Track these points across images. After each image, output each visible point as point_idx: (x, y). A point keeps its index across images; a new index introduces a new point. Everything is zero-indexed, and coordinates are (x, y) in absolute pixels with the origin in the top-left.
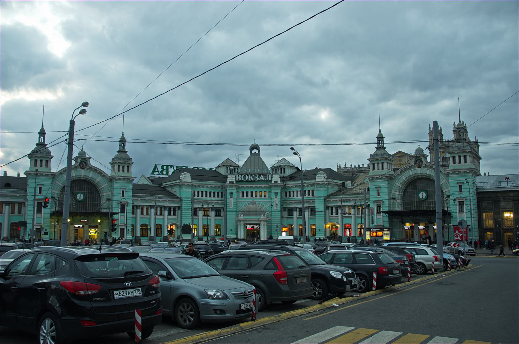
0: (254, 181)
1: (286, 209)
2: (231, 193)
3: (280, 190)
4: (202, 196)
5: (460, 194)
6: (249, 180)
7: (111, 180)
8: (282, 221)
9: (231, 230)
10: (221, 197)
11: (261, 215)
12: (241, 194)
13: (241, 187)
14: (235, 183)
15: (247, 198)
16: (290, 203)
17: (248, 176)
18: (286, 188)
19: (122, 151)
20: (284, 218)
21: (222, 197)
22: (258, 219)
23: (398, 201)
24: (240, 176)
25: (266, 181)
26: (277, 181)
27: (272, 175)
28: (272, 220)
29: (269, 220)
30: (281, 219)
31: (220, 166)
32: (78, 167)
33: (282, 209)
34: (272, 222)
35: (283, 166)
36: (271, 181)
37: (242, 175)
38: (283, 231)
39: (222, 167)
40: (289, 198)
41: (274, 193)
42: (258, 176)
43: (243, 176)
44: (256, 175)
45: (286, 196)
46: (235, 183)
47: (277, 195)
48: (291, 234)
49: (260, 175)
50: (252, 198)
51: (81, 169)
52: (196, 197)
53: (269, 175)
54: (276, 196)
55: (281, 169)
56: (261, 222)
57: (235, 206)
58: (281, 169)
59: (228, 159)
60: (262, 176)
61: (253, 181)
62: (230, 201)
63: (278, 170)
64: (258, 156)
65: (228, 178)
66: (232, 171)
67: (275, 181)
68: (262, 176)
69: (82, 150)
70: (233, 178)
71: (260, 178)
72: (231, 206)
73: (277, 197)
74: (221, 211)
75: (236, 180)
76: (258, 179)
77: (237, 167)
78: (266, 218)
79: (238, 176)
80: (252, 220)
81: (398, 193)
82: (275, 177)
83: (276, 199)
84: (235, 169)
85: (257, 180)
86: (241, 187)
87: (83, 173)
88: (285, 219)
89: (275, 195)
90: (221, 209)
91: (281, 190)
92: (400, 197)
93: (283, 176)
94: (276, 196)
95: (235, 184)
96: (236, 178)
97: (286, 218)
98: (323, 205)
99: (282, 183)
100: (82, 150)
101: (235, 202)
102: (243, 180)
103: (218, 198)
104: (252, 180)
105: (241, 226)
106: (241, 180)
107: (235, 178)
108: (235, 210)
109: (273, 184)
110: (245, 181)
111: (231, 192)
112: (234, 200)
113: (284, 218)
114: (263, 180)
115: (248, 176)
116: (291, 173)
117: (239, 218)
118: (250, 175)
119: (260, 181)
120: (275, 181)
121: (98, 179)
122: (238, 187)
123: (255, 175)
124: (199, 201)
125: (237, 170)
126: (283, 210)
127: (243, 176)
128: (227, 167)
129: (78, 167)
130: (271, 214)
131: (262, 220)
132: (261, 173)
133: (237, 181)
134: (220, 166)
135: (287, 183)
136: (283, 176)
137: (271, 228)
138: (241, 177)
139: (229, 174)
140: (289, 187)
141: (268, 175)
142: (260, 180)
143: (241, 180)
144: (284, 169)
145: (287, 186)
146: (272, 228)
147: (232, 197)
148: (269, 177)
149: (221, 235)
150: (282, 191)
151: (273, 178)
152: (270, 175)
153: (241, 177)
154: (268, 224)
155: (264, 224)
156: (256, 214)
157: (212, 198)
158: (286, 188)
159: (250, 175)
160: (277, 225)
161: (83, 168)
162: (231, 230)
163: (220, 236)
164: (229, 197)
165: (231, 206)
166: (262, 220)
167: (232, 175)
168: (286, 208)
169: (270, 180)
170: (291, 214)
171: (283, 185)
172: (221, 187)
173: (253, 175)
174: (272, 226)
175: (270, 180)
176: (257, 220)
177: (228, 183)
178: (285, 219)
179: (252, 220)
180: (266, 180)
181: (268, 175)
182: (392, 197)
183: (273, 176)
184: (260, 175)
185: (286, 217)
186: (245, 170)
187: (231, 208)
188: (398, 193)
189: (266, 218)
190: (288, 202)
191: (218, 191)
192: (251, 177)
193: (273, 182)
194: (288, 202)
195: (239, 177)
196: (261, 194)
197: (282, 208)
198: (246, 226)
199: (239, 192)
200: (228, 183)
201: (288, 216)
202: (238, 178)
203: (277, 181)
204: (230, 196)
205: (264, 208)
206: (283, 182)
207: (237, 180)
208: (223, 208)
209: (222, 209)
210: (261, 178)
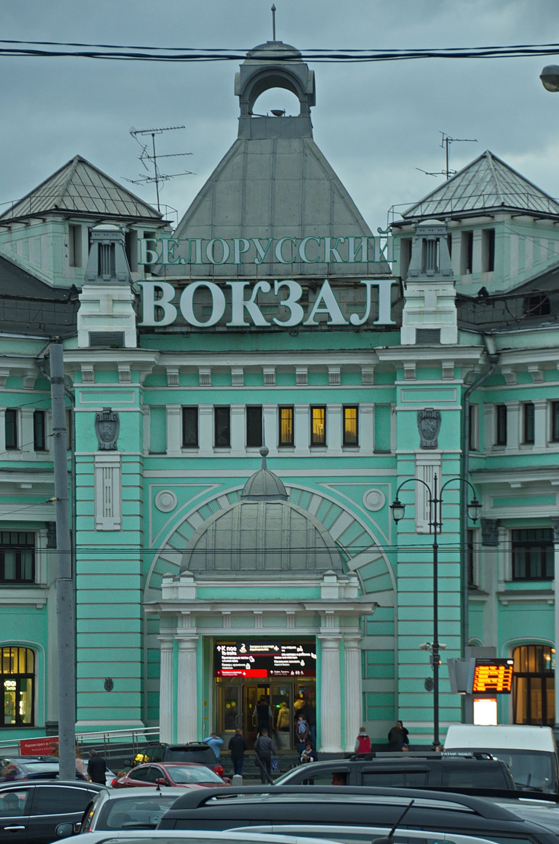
1: (497, 535)
3: (457, 394)
6: (238, 320)
8: (471, 617)
9: (109, 685)
10: (36, 448)
11: (322, 574)
13: (175, 372)
14: (131, 341)
15: (222, 452)
16: (526, 485)
17: (226, 289)
18: (500, 379)
20: (486, 594)
21: (39, 446)
22: (301, 604)
24: (169, 291)
25: (357, 329)
26: (438, 331)
28: (402, 613)
29: (379, 614)
30: (463, 607)
31: (25, 219)
33: (471, 532)
34: (402, 628)
35: (484, 212)
36: (396, 328)
37: (180, 286)
38: (482, 688)
39: (34, 222)
40: (527, 450)
41: (414, 417)
42: (296, 291)
43: (190, 291)
44: (285, 287)
45: (502, 440)
46: (131, 341)
47: (436, 430)
48: (538, 714)
50: (255, 452)
53: (375, 287)
55: (469, 238)
56: (318, 625)
57: (136, 508)
58: (469, 238)
59: (82, 161)
60: (326, 290)
61: (262, 331)
62: (99, 473)
63: (443, 244)
64: (296, 144)
65: (83, 310)
66: (106, 254)
67: (419, 331)
68: (326, 290)
70: (119, 309)
71: (315, 309)
72: (108, 512)
73: (435, 447)
74: (31, 549)
75: (139, 318)
76: (294, 320)
77: (151, 227)
78: (354, 594)
79: (158, 289)
80: (258, 610)
82: (422, 298)
84: (130, 237)
85: (293, 321)
86: (175, 372)
88: (492, 600)
89: (423, 432)
90: (33, 534)
91: (465, 395)
93: (483, 291)
95: (131, 350)
97: (499, 594)
99: (475, 340)
101: (136, 480)
102: (191, 319)
103: (13, 455)
104: (260, 320)
105: (181, 656)
106: (180, 321)
107: (130, 311)
108: (136, 538)
109: (408, 348)
110: (202, 331)
112: (127, 468)
113: (486, 594)
114: (338, 318)
115: (226, 289)
116: (543, 267)
117: (166, 595)
118: (238, 288)
119: (311, 328)
120: (419, 331)
123: (277, 285)
125: (142, 245)
126: (478, 538)
127: (190, 291)
128: (75, 221)
130: (395, 571)
131: (330, 610)
132: (316, 271)
133: (150, 330)
134: (25, 219)
135: (506, 342)
136: (483, 291)
137: (393, 665)
138: (176, 303)
139: (91, 281)
140: (516, 367)
141: (369, 283)
142: (310, 321)
143: (180, 321)
144: (490, 235)
145: (506, 361)
146: (402, 671)
147: (115, 449)
148: (376, 303)
149: (40, 722)
150: (472, 399)
151: (408, 306)
152: (385, 287)
153: (176, 303)
154: (369, 643)
155: (342, 642)
156: (281, 571)
158: (500, 379)
159: (238, 288)
160: (436, 646)
162: (109, 685)
163: (31, 725)
164: (95, 442)
165: (108, 512)
166: (330, 610)
167: (107, 282)
168: (499, 522)
169: (385, 318)
170: (536, 570)
171: (476, 355)
172: (30, 375)
173: (265, 286)
174: (402, 657)
175: (385, 318)
176: (290, 610)
177: (83, 341)
178: (492, 600)
179: (258, 610)
180: (355, 320)
181: (369, 283)
183: (410, 290)
185: (502, 588)
186: (203, 250)
187: (108, 523)
189: (354, 594)
190: (516, 481)
191: (12, 405)
192: (247, 298)
194: (516, 481)
195: (164, 303)
196: (318, 425)
197: (471, 524)
198: (218, 655)
199: (163, 408)
200: (83, 341)
201: (515, 579)
202: (158, 308)
203: (438, 331)
204: (102, 437)
205: (344, 521)
206: (483, 335)
207: (149, 320)
208: (50, 526)
209: (44, 531)
210: (323, 305)
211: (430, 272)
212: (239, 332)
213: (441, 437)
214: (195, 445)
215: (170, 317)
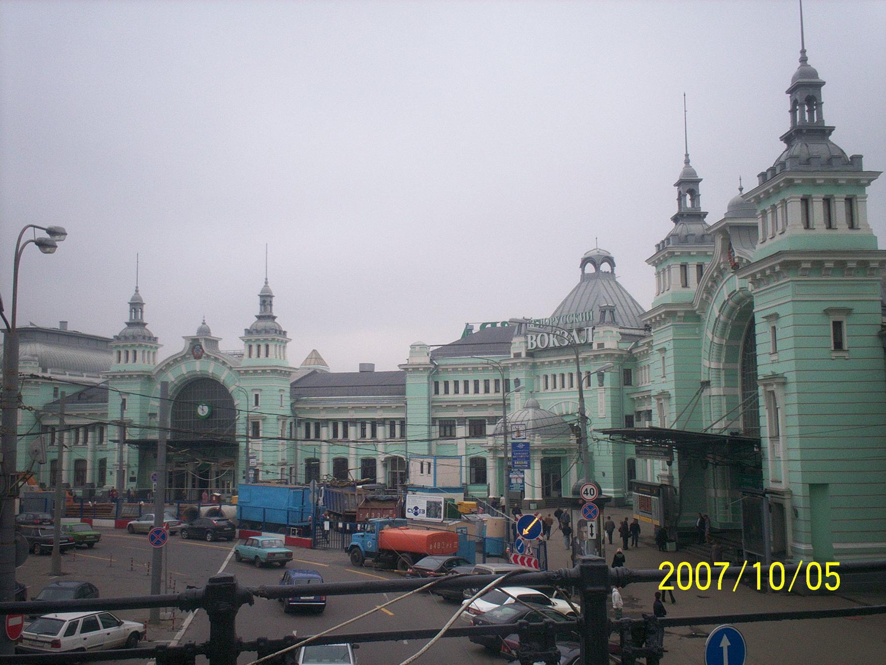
0: (561, 348)
2: (517, 381)
4: (457, 392)
5: (773, 362)
6: (551, 345)
7: (245, 373)
12: (542, 381)
14: (523, 355)
19: (266, 315)
21: (497, 391)
23: (714, 391)
27: (593, 329)
32: (187, 356)
36: (591, 344)
49: (570, 331)
51: (195, 358)
52: (442, 394)
53: (587, 330)
54: (601, 383)
67: (598, 344)
68: (574, 333)
69: (204, 323)
73: (602, 385)
75: (527, 347)
81: (713, 365)
83: (601, 390)
85: (566, 344)
87: (198, 366)
92: (723, 378)
94: (601, 383)
96: (527, 342)
98: (426, 415)
100: (204, 323)
102: (540, 346)
107: (523, 345)
111: (517, 379)
114: (578, 342)
121: (224, 376)
122: (534, 366)
124: (452, 406)
129: (187, 356)
141: (586, 328)
152: (590, 329)
157: (482, 395)
161: (198, 358)
169: (590, 341)
177: (512, 357)
180: (583, 342)
181: (586, 328)
182: (702, 380)
184: (570, 331)
188: (713, 365)
193: (595, 346)
202: (532, 344)
203: (603, 344)
207: (530, 348)
211: (602, 323)
212: (552, 349)
213: (605, 382)
214: (458, 393)
215: (534, 346)
